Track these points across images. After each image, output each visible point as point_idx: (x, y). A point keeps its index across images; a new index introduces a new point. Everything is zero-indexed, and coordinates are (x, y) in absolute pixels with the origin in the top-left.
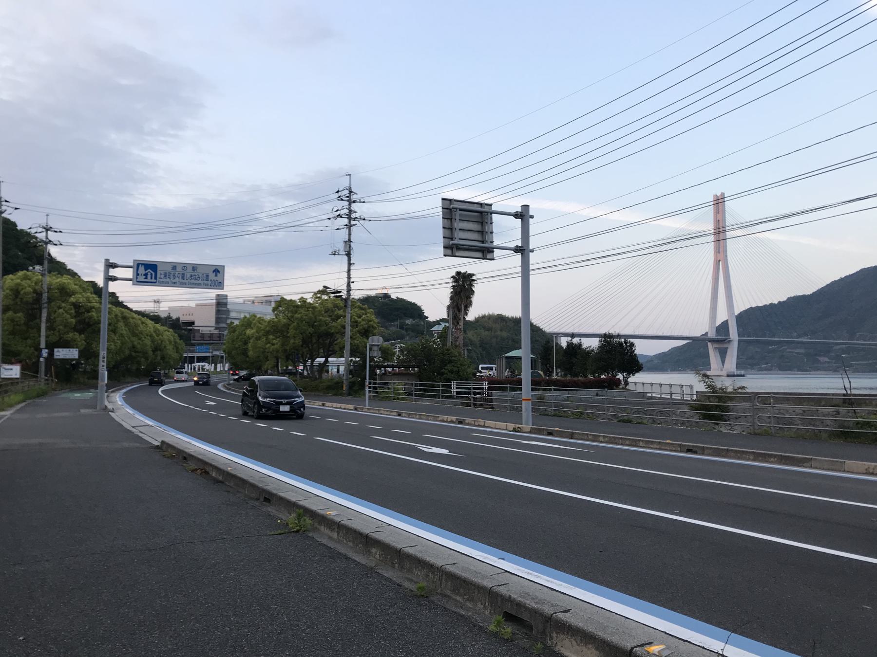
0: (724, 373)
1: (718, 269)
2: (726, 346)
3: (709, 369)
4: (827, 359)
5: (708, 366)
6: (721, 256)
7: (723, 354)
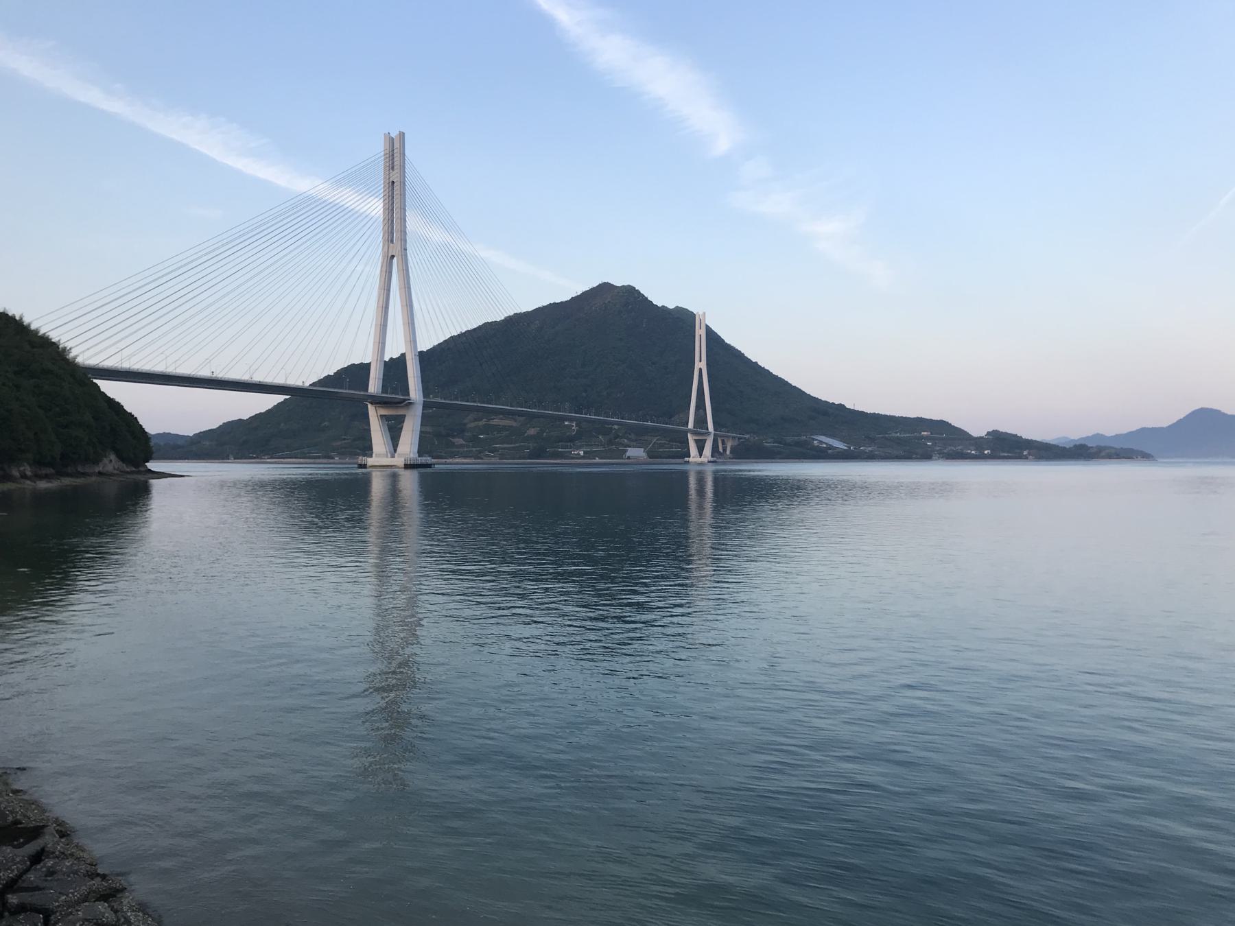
0: (399, 461)
1: (391, 272)
2: (400, 412)
3: (371, 456)
4: (461, 441)
5: (368, 450)
6: (395, 249)
7: (394, 430)
